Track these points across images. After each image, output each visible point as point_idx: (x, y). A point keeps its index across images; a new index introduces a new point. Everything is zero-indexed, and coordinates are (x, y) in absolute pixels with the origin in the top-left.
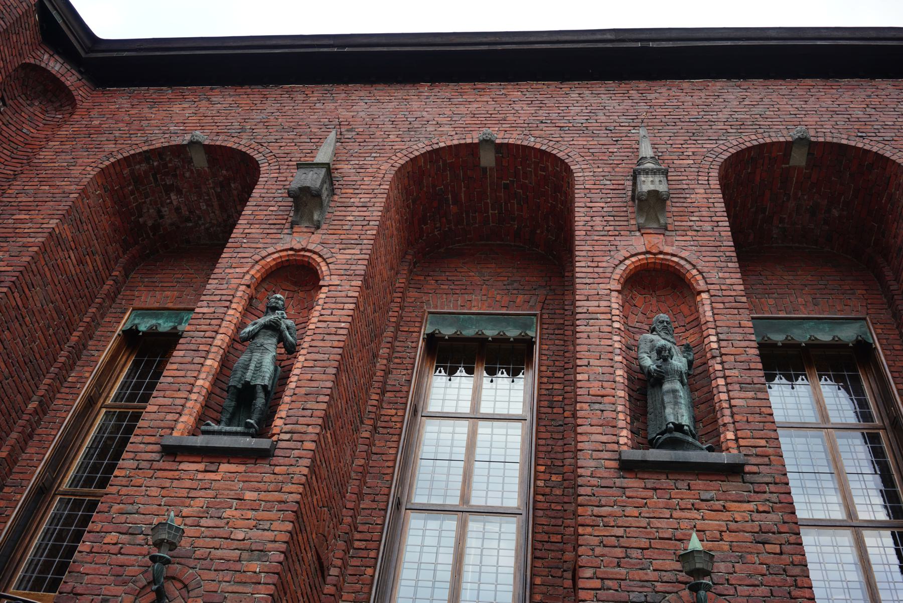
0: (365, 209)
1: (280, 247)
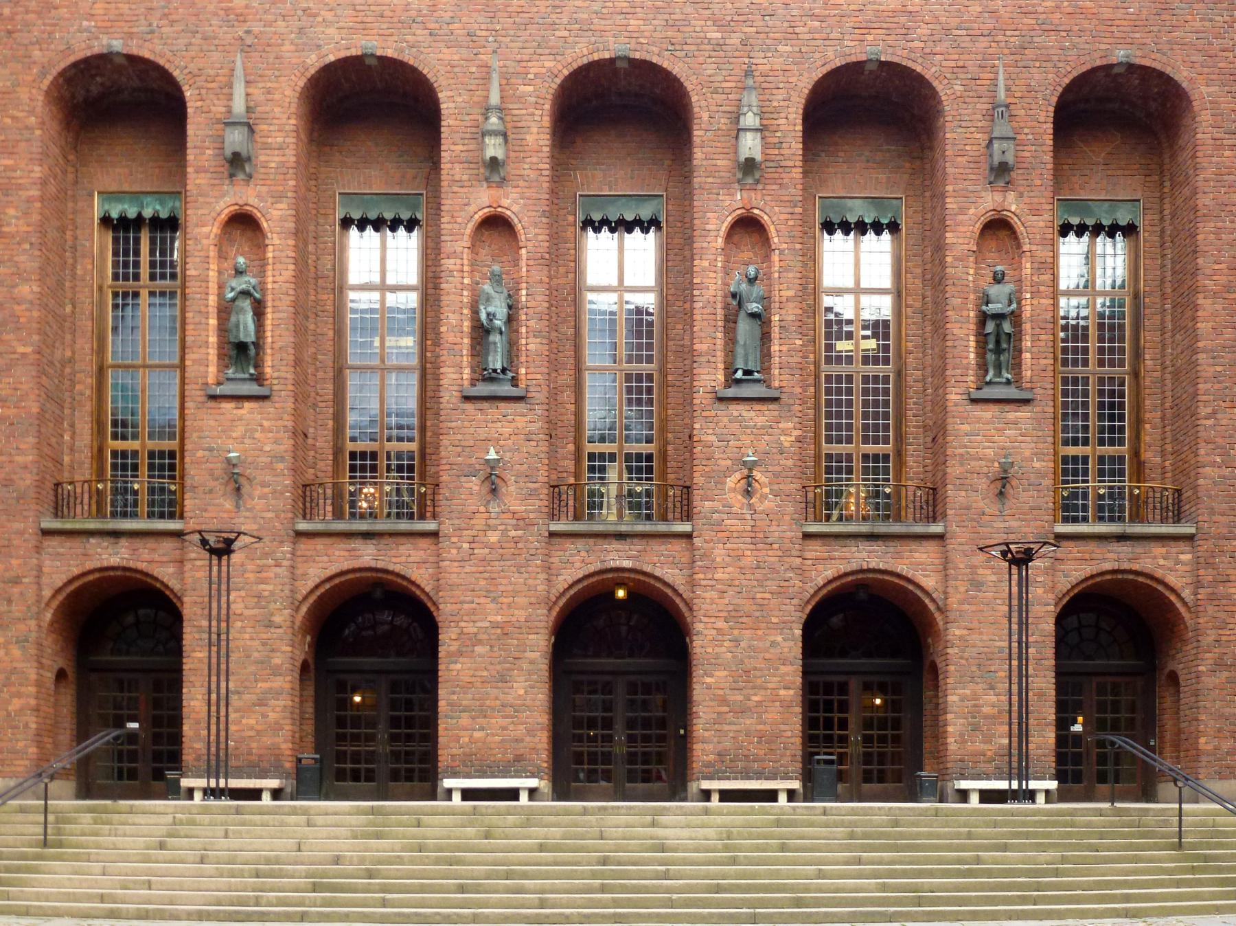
0: (281, 152)
1: (228, 200)
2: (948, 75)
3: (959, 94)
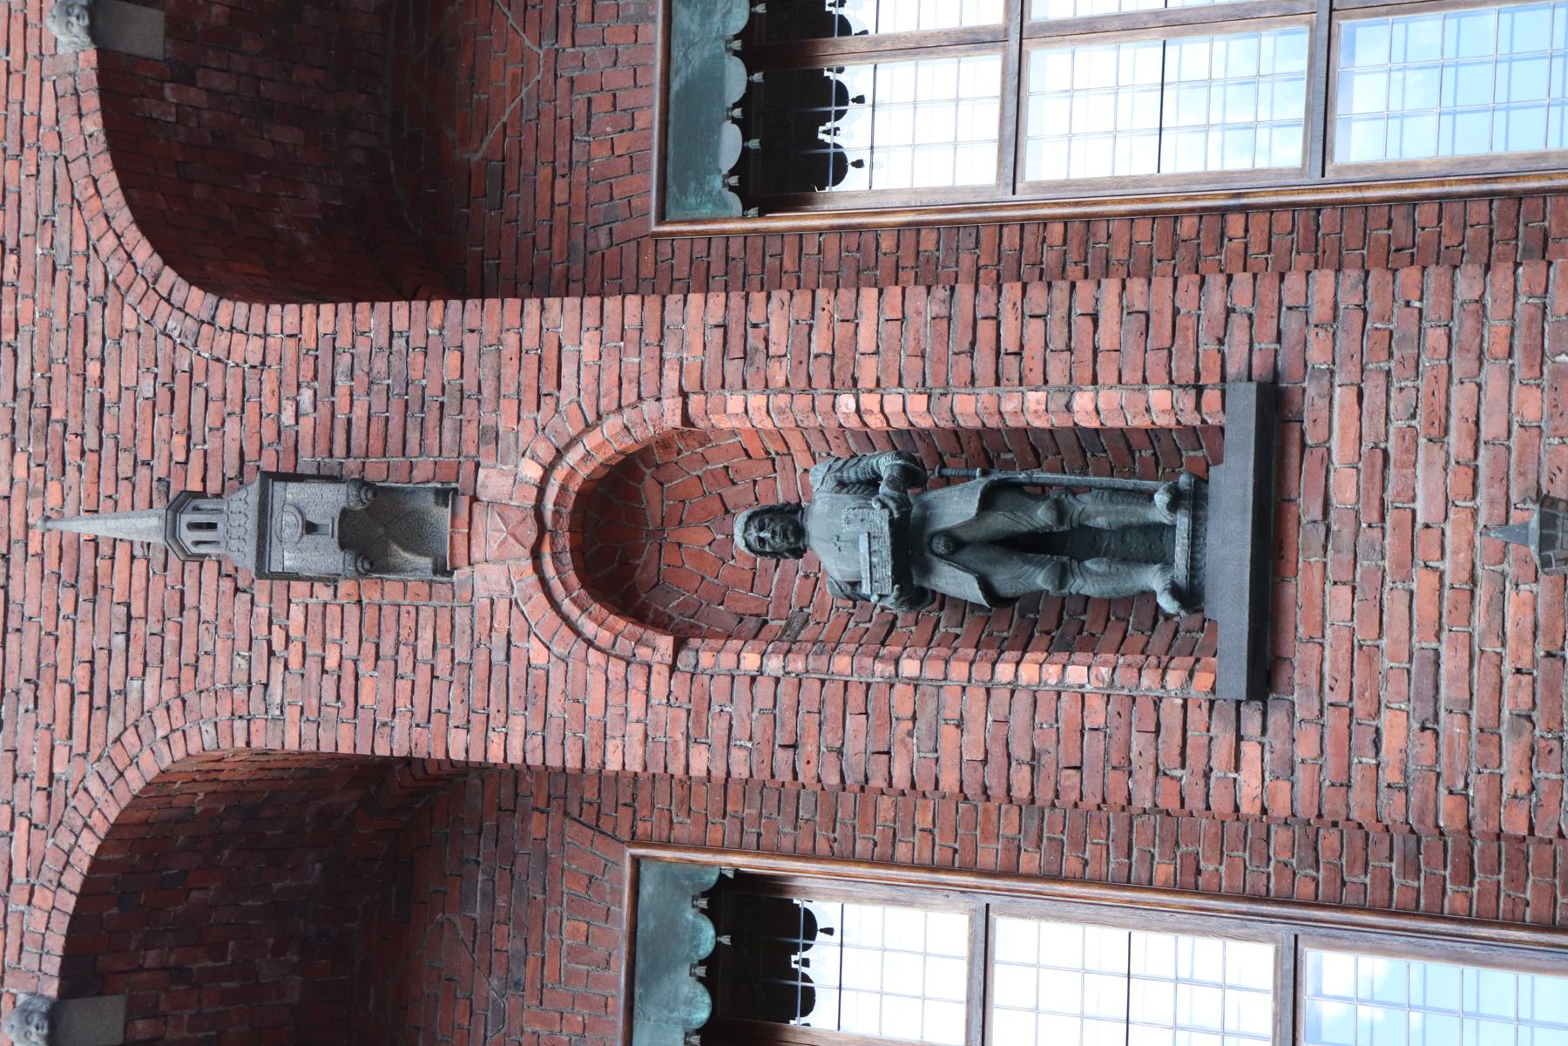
2: (114, 728)
3: (169, 689)
